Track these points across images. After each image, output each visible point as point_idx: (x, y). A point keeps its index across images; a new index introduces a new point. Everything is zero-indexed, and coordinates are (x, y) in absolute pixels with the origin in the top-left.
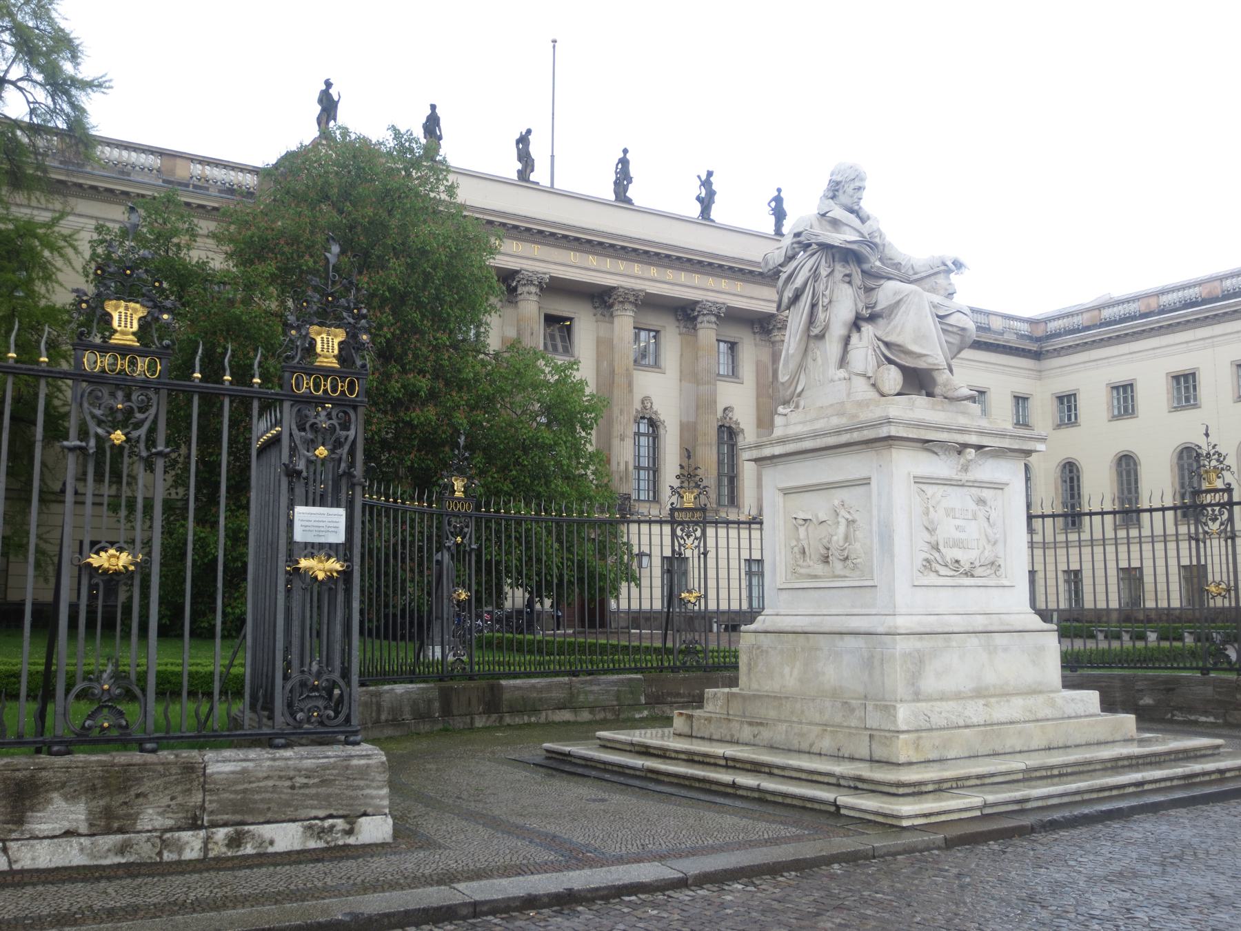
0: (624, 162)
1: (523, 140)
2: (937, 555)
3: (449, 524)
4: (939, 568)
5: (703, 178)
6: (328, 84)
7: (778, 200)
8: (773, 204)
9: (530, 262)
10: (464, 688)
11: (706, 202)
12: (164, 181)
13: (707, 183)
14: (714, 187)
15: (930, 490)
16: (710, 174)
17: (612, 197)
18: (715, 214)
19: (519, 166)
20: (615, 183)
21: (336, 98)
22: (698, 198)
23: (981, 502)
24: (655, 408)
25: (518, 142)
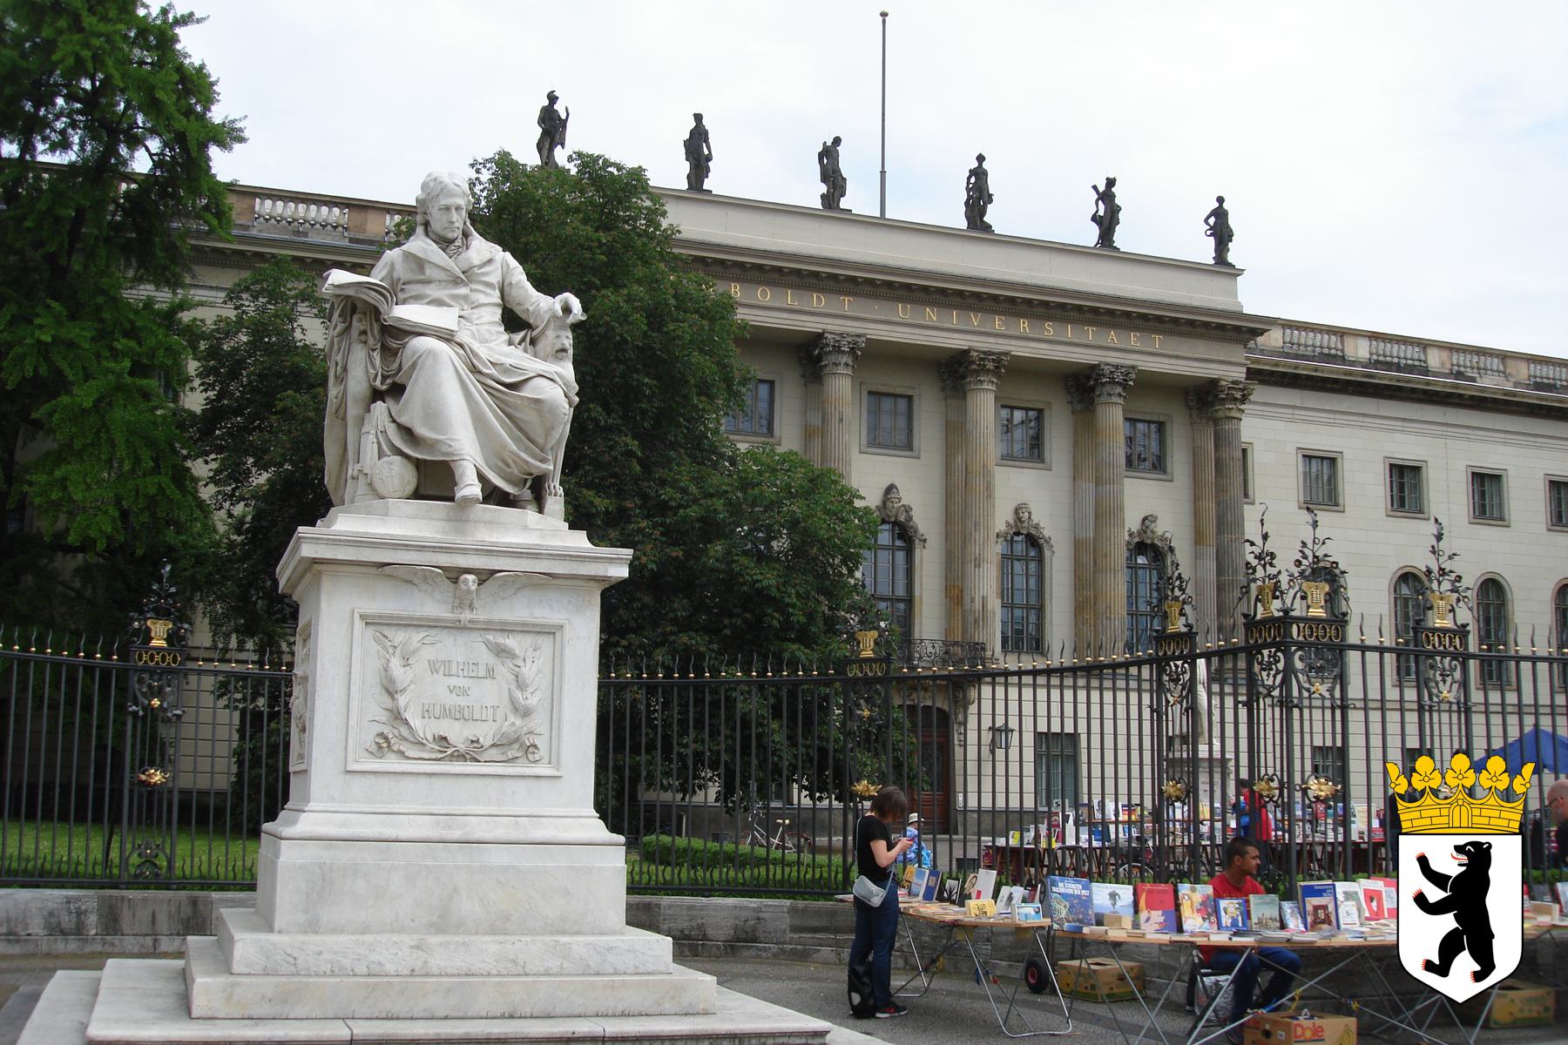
0: (979, 175)
1: (829, 155)
2: (405, 732)
3: (141, 681)
5: (1102, 188)
6: (552, 98)
7: (1220, 214)
8: (1212, 221)
9: (837, 321)
10: (145, 900)
11: (1107, 222)
12: (352, 240)
13: (1107, 196)
14: (1117, 201)
15: (399, 636)
16: (1111, 183)
17: (963, 224)
18: (1122, 239)
19: (824, 189)
20: (967, 203)
21: (563, 116)
22: (1095, 218)
23: (501, 652)
24: (1035, 519)
25: (821, 156)
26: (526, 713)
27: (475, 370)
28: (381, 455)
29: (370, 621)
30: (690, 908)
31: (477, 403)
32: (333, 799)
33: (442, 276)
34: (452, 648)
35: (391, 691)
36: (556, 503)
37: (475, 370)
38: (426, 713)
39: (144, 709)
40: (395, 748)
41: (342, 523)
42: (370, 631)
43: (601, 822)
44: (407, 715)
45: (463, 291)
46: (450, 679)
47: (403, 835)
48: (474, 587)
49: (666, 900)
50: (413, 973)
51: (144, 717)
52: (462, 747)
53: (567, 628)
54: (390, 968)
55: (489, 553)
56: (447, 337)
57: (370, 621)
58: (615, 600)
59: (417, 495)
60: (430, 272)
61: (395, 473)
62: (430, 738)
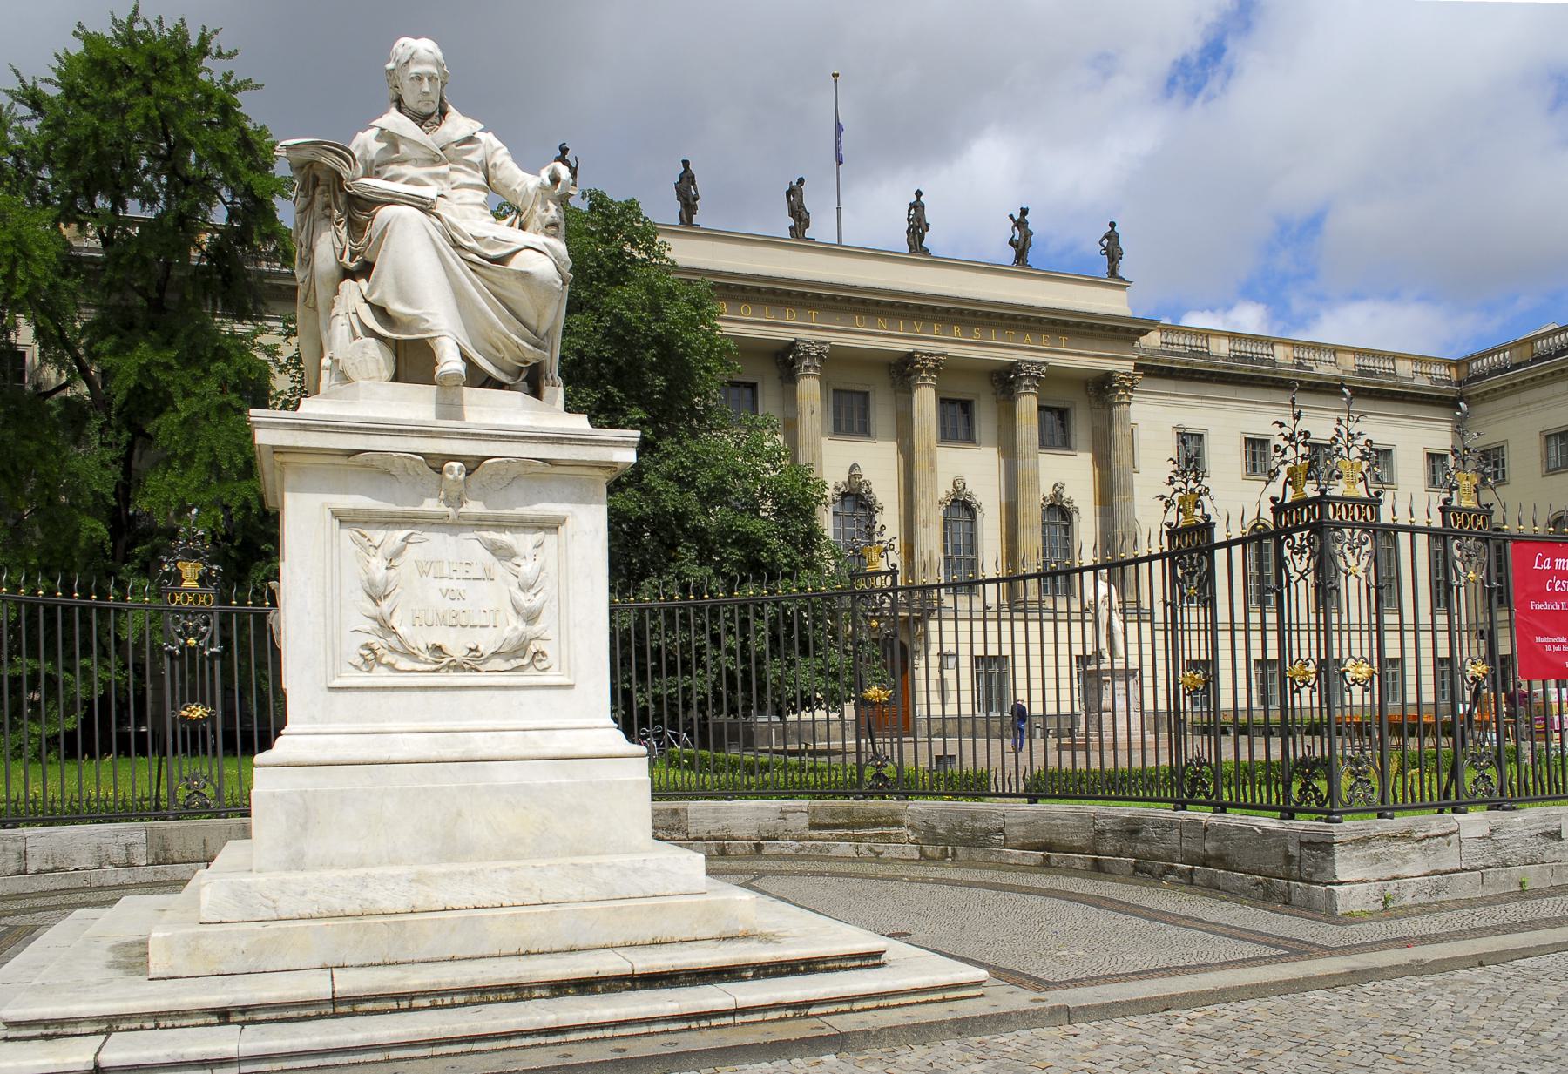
2: (393, 640)
15: (378, 535)
26: (531, 617)
27: (457, 246)
28: (355, 337)
29: (345, 519)
30: (716, 811)
31: (456, 275)
32: (313, 719)
34: (437, 544)
36: (556, 393)
37: (457, 246)
38: (417, 622)
39: (182, 649)
40: (384, 660)
41: (310, 408)
42: (346, 533)
43: (620, 734)
44: (394, 622)
47: (396, 756)
48: (462, 476)
49: (692, 805)
51: (182, 656)
53: (569, 521)
57: (345, 519)
58: (620, 483)
59: (396, 378)
61: (374, 358)
62: (423, 647)
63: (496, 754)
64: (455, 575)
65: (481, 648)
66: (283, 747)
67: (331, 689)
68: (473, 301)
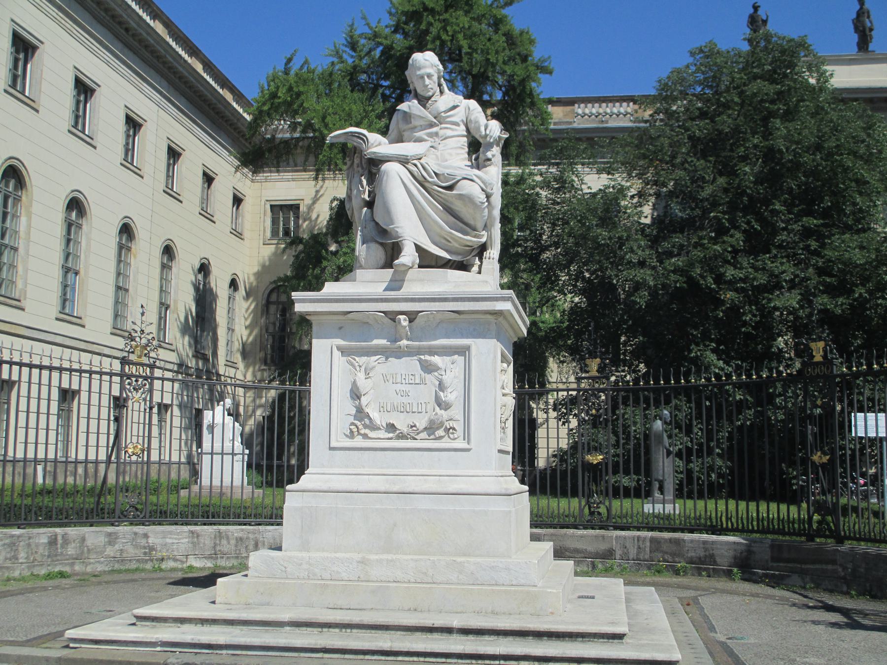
4: (367, 431)
6: (756, 8)
15: (363, 360)
29: (344, 351)
33: (422, 123)
35: (356, 394)
38: (382, 409)
44: (367, 410)
45: (434, 129)
46: (392, 385)
50: (359, 580)
52: (405, 430)
54: (344, 575)
55: (413, 300)
56: (404, 161)
60: (415, 122)
63: (417, 490)
64: (404, 381)
65: (418, 425)
66: (305, 481)
67: (331, 449)
68: (429, 216)
